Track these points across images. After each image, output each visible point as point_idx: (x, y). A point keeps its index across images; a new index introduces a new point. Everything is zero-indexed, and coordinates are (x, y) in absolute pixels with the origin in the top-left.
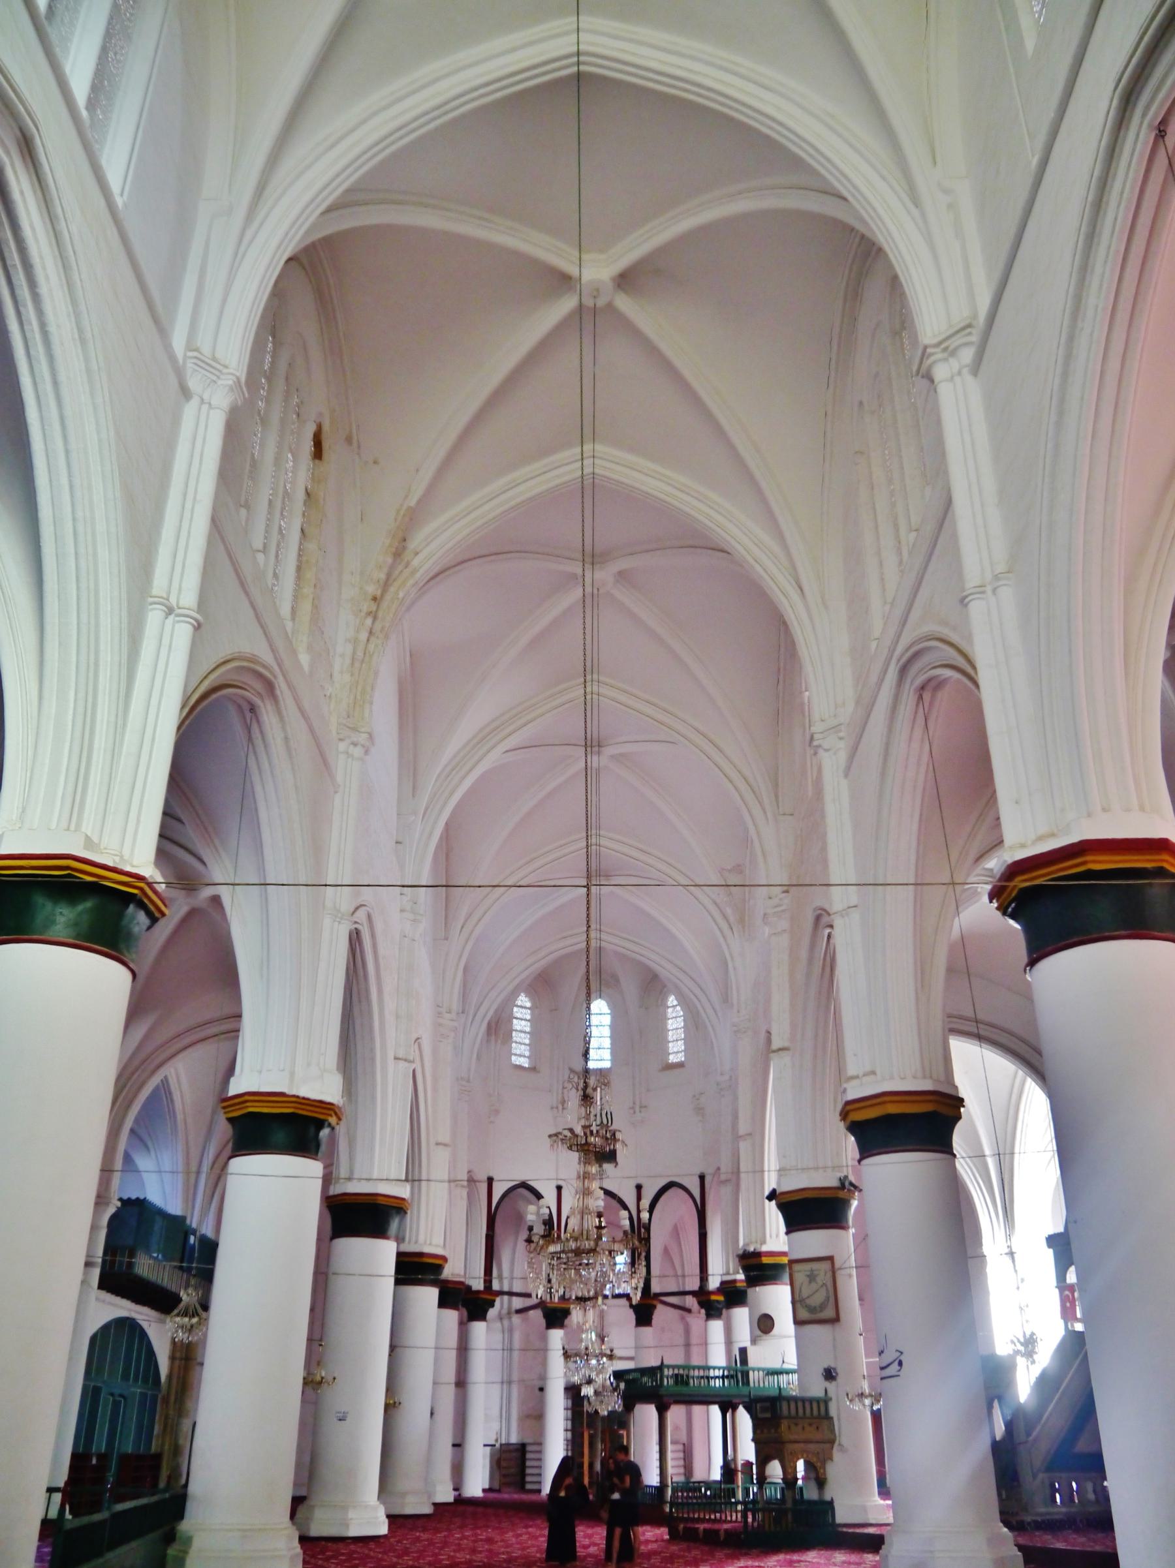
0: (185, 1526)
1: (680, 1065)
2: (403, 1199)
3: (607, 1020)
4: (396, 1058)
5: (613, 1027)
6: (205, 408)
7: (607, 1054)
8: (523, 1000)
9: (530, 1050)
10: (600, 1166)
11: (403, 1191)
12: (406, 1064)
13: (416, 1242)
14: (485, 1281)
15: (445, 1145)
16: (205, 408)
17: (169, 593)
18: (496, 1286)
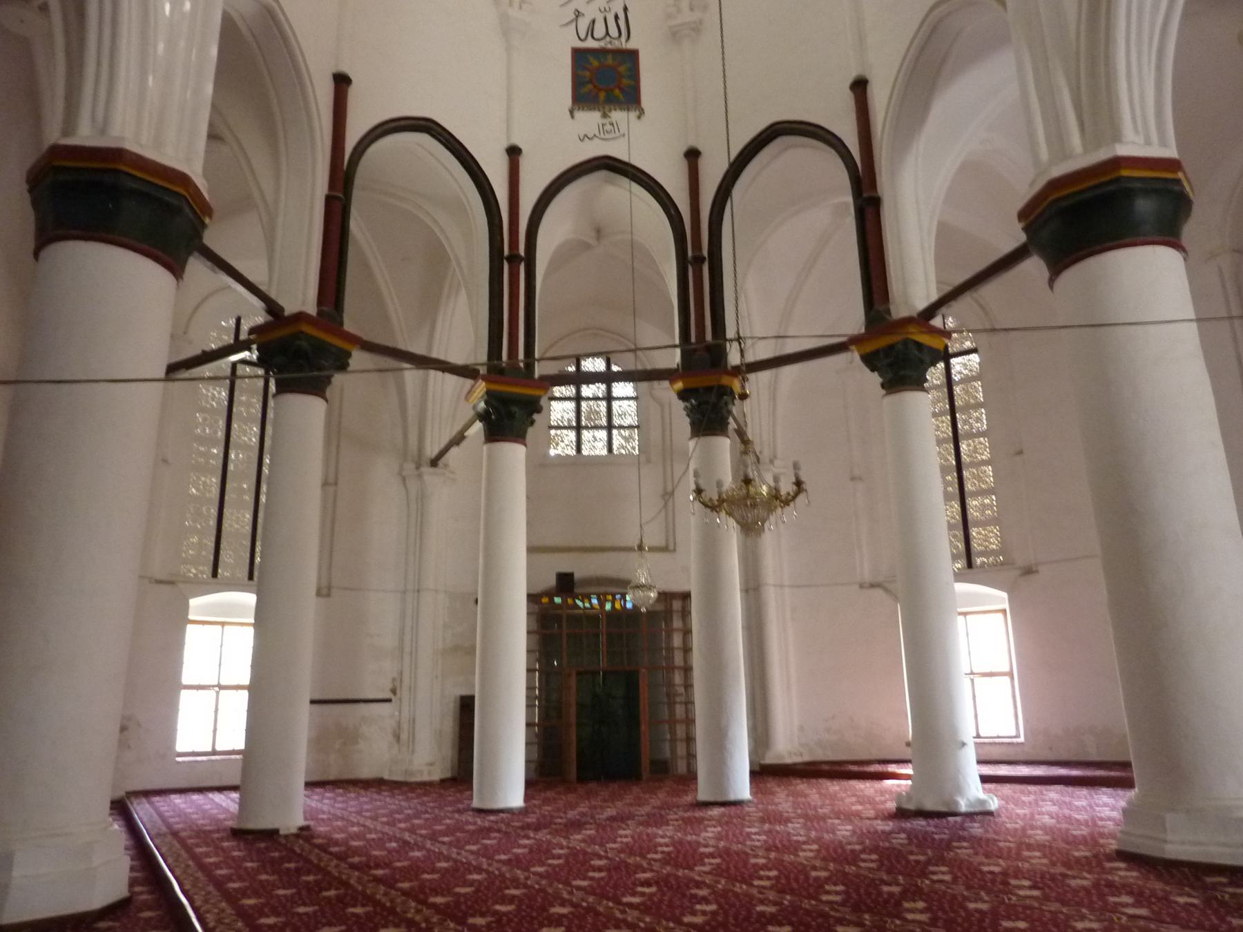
10: (605, 116)
14: (321, 301)
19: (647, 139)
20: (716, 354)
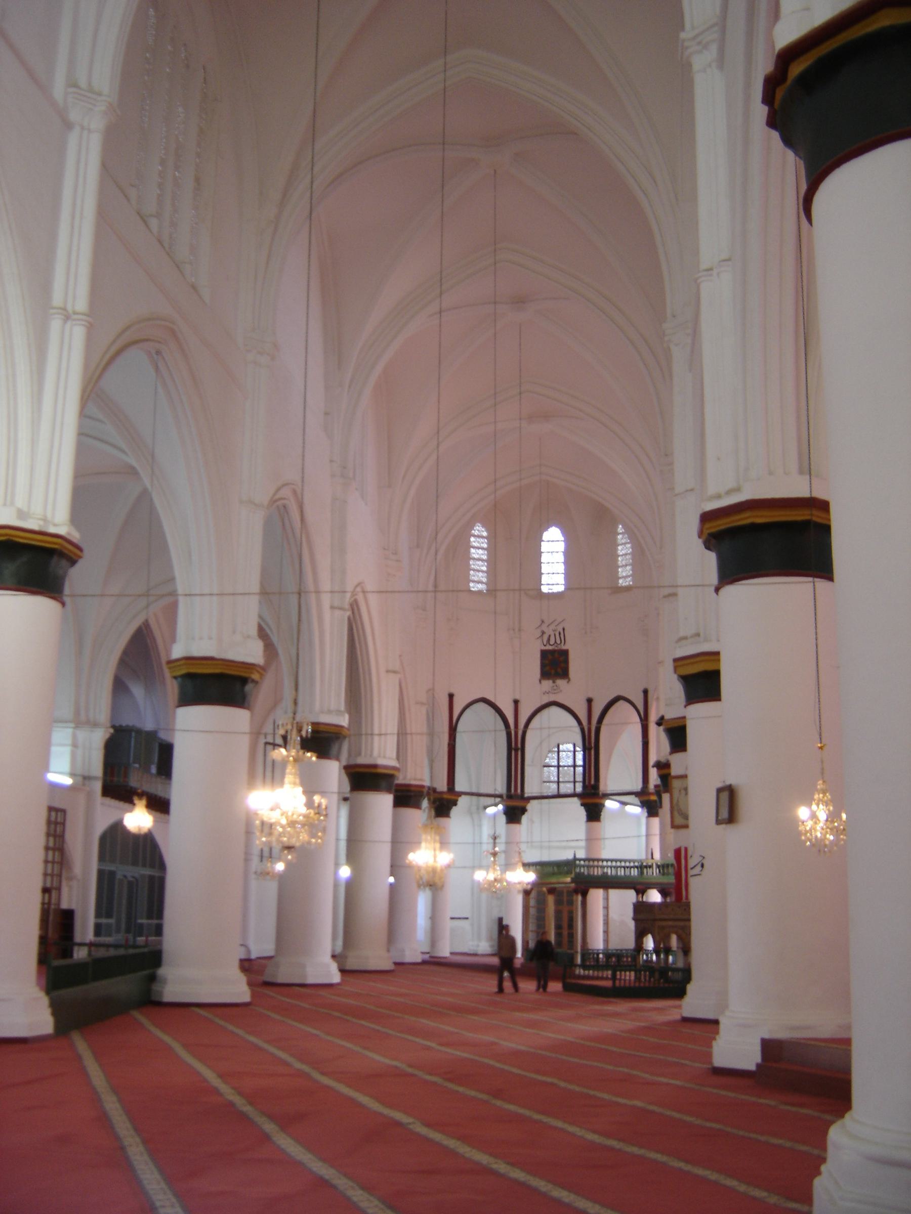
0: (162, 971)
1: (628, 589)
2: (342, 727)
3: (561, 546)
4: (332, 607)
5: (566, 553)
6: (85, 132)
7: (561, 579)
8: (479, 529)
9: (488, 577)
10: (554, 682)
11: (344, 721)
12: (341, 612)
13: (371, 755)
14: (448, 784)
15: (395, 672)
16: (85, 132)
17: (66, 302)
18: (458, 788)
19: (572, 691)
20: (596, 786)
